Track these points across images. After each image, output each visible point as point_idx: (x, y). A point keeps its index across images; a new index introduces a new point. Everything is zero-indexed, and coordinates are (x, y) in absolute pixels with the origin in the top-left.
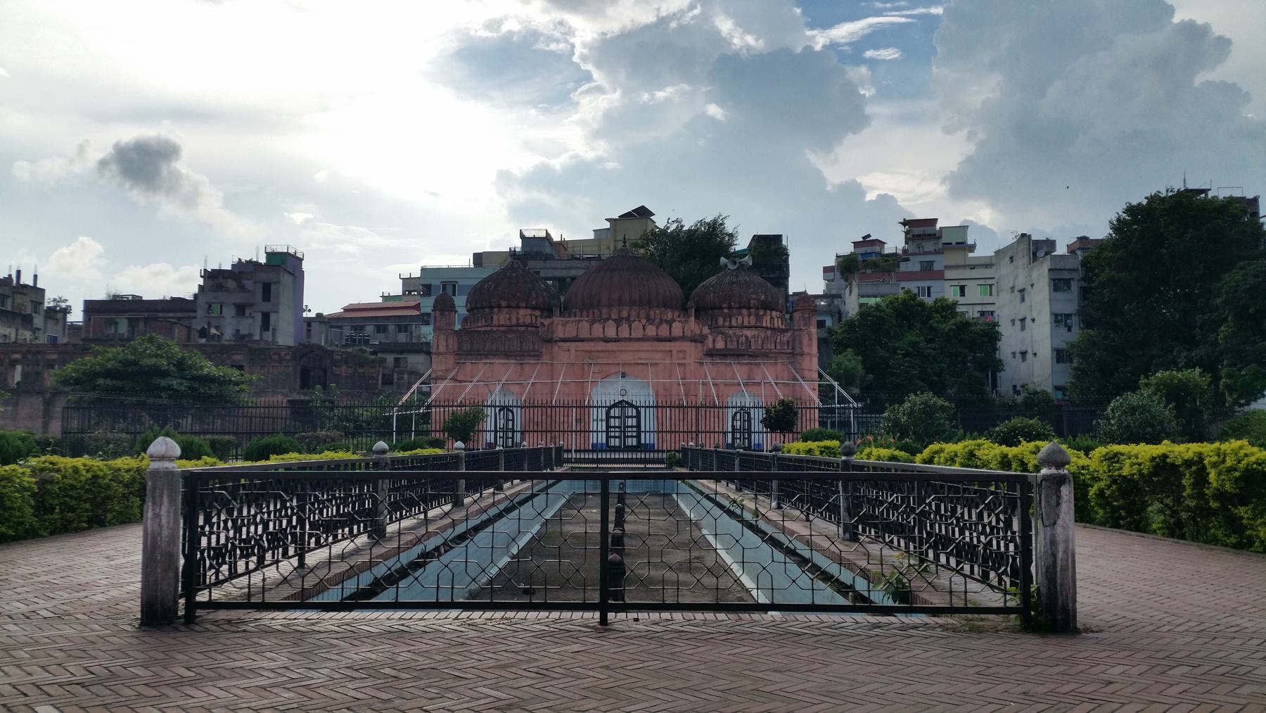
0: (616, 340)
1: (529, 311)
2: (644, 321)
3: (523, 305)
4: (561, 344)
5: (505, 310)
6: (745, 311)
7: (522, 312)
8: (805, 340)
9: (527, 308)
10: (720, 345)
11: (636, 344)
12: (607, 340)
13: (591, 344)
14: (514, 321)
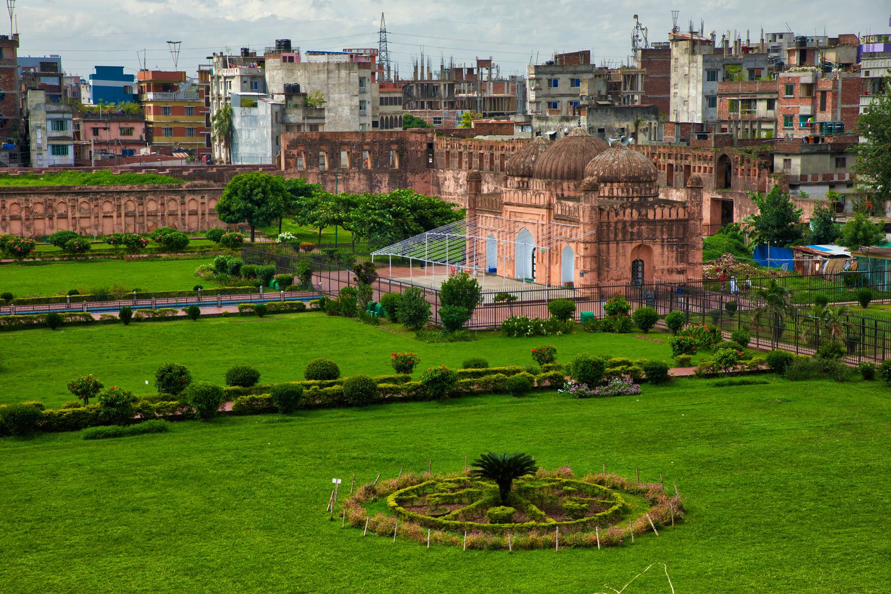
1: (520, 179)
9: (518, 176)
10: (559, 213)
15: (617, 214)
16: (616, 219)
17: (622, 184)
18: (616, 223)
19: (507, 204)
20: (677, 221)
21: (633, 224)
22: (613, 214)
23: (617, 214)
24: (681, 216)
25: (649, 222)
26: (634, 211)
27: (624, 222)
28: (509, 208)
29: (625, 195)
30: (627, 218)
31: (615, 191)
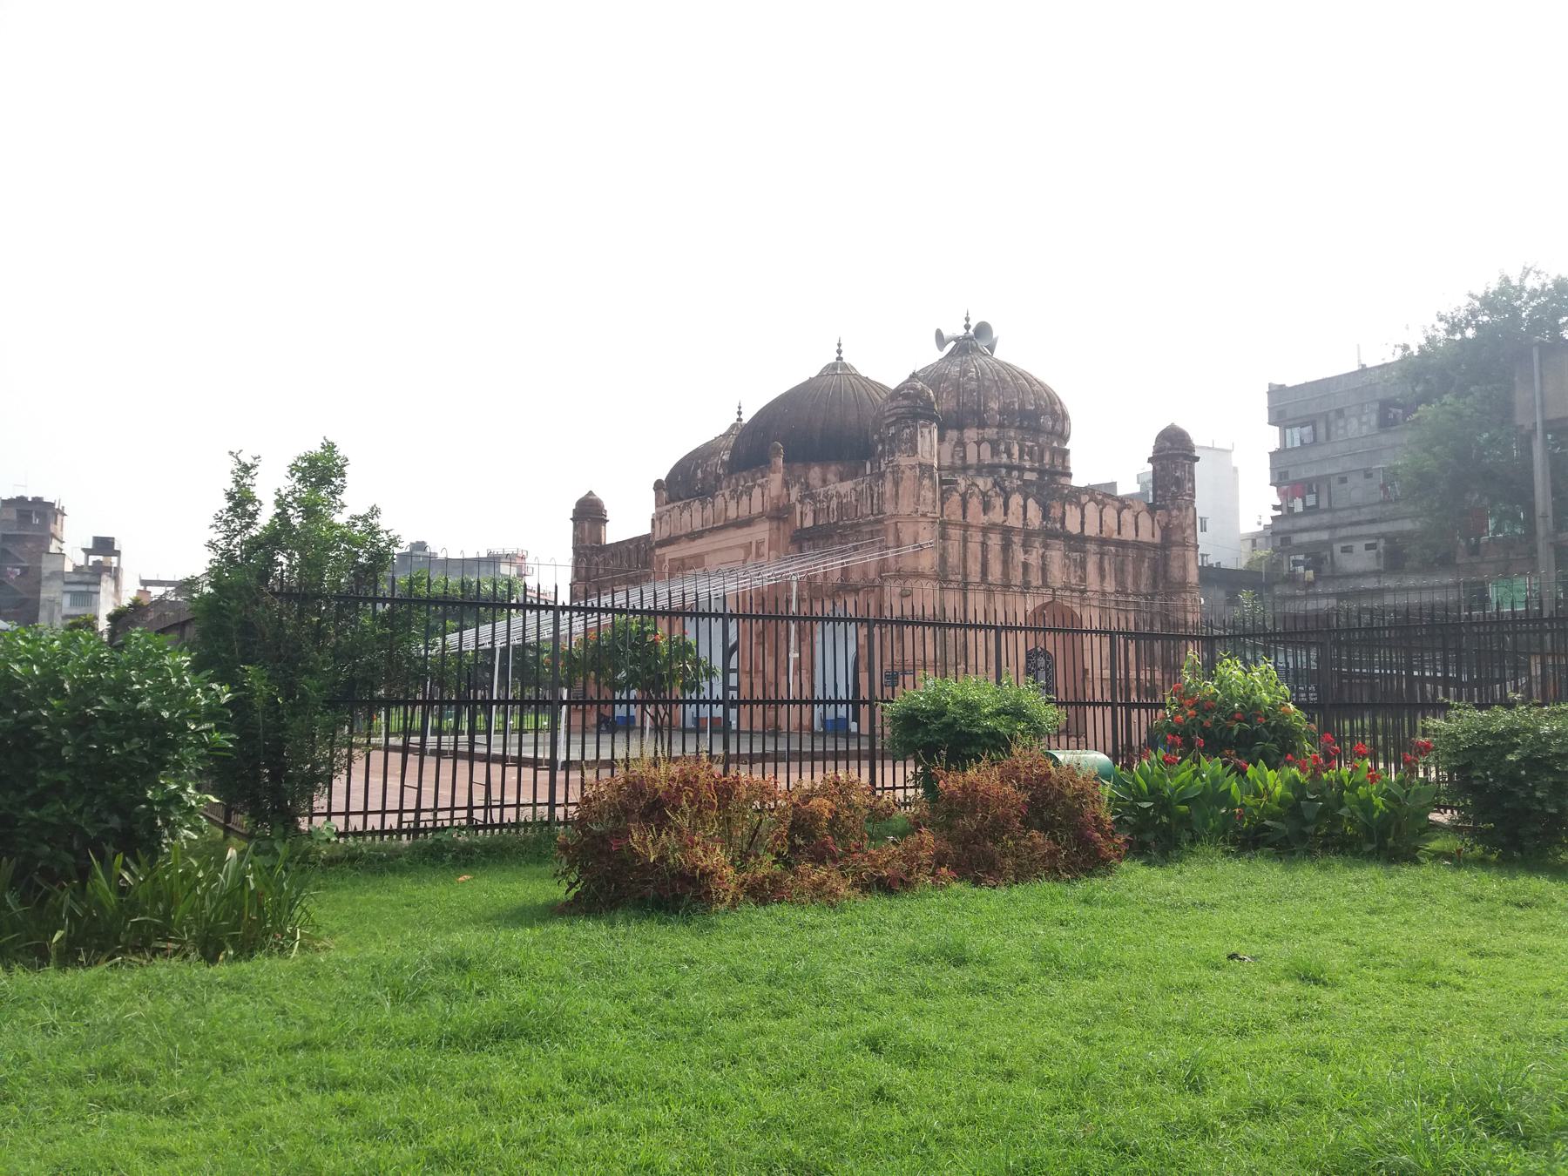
4: (658, 552)
10: (808, 523)
12: (694, 536)
15: (987, 507)
16: (984, 519)
17: (991, 433)
18: (986, 530)
20: (1138, 546)
21: (1028, 535)
22: (975, 504)
23: (987, 507)
24: (1145, 536)
25: (1068, 537)
26: (1031, 503)
27: (1006, 532)
29: (1004, 458)
30: (1014, 521)
31: (972, 451)
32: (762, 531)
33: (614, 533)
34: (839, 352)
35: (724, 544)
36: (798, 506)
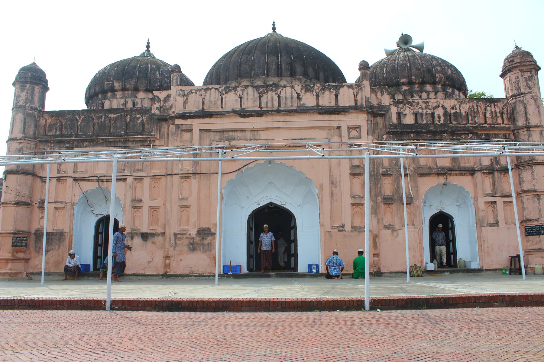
0: (260, 114)
2: (298, 88)
3: (142, 87)
4: (178, 122)
5: (119, 94)
6: (429, 88)
7: (141, 95)
8: (531, 109)
10: (409, 120)
11: (288, 118)
12: (243, 114)
13: (226, 120)
14: (130, 105)
19: (185, 116)
28: (198, 124)
32: (360, 119)
33: (52, 103)
34: (274, 29)
35: (297, 125)
36: (394, 110)
